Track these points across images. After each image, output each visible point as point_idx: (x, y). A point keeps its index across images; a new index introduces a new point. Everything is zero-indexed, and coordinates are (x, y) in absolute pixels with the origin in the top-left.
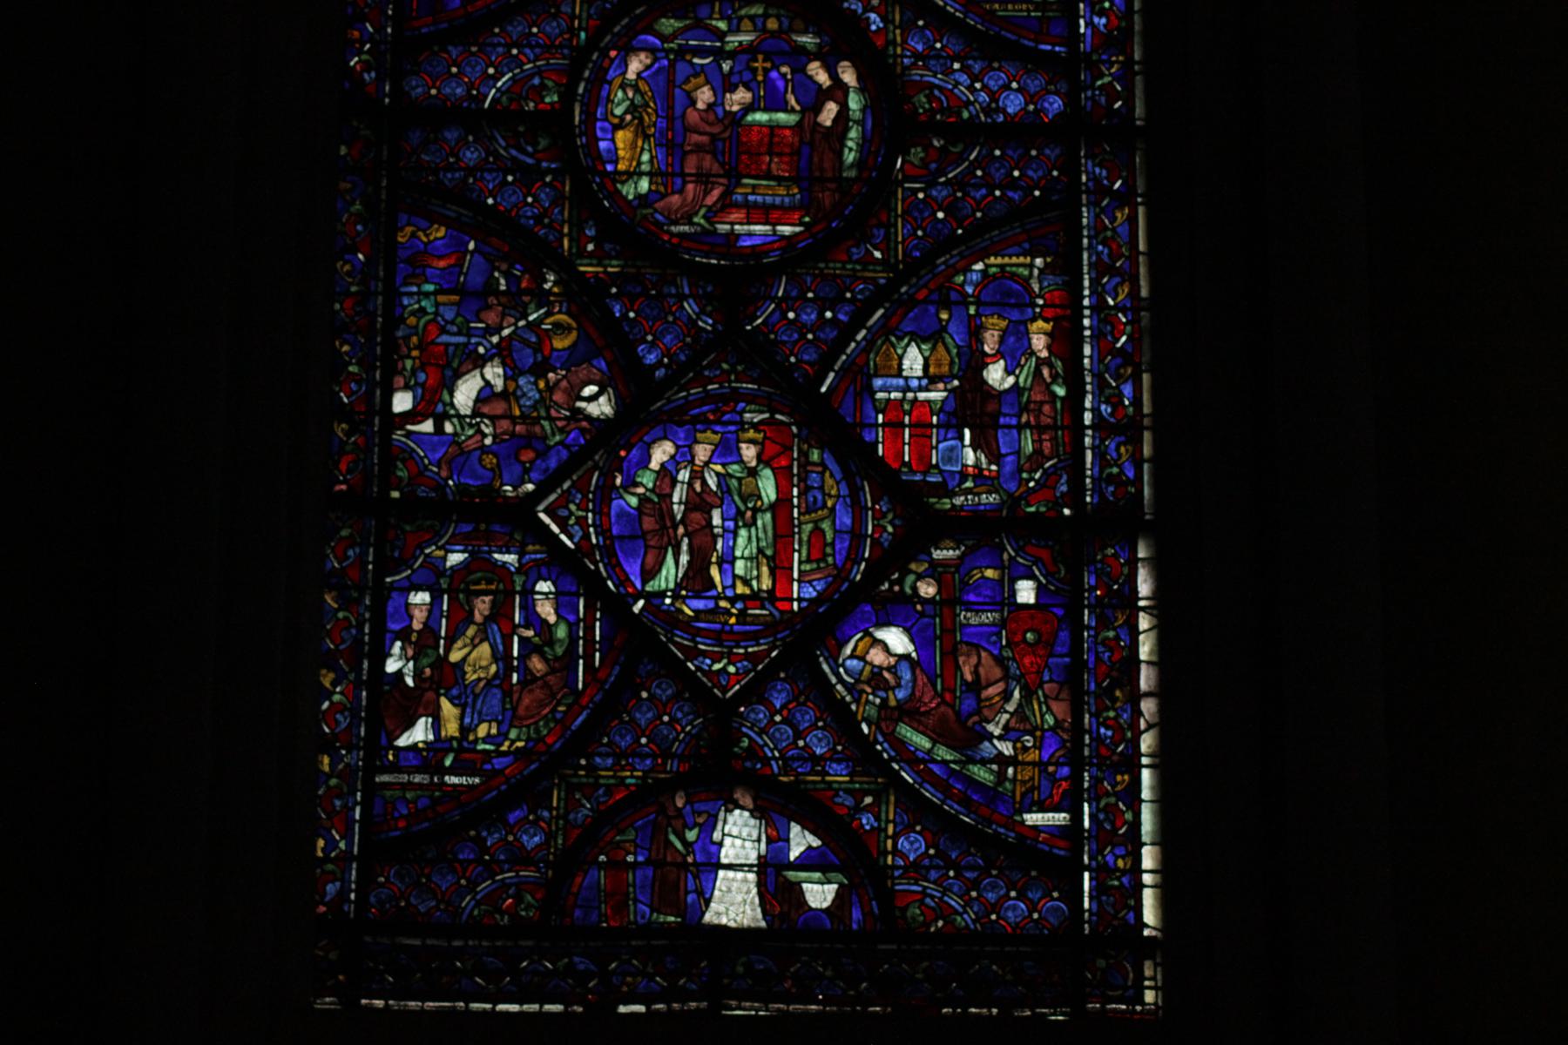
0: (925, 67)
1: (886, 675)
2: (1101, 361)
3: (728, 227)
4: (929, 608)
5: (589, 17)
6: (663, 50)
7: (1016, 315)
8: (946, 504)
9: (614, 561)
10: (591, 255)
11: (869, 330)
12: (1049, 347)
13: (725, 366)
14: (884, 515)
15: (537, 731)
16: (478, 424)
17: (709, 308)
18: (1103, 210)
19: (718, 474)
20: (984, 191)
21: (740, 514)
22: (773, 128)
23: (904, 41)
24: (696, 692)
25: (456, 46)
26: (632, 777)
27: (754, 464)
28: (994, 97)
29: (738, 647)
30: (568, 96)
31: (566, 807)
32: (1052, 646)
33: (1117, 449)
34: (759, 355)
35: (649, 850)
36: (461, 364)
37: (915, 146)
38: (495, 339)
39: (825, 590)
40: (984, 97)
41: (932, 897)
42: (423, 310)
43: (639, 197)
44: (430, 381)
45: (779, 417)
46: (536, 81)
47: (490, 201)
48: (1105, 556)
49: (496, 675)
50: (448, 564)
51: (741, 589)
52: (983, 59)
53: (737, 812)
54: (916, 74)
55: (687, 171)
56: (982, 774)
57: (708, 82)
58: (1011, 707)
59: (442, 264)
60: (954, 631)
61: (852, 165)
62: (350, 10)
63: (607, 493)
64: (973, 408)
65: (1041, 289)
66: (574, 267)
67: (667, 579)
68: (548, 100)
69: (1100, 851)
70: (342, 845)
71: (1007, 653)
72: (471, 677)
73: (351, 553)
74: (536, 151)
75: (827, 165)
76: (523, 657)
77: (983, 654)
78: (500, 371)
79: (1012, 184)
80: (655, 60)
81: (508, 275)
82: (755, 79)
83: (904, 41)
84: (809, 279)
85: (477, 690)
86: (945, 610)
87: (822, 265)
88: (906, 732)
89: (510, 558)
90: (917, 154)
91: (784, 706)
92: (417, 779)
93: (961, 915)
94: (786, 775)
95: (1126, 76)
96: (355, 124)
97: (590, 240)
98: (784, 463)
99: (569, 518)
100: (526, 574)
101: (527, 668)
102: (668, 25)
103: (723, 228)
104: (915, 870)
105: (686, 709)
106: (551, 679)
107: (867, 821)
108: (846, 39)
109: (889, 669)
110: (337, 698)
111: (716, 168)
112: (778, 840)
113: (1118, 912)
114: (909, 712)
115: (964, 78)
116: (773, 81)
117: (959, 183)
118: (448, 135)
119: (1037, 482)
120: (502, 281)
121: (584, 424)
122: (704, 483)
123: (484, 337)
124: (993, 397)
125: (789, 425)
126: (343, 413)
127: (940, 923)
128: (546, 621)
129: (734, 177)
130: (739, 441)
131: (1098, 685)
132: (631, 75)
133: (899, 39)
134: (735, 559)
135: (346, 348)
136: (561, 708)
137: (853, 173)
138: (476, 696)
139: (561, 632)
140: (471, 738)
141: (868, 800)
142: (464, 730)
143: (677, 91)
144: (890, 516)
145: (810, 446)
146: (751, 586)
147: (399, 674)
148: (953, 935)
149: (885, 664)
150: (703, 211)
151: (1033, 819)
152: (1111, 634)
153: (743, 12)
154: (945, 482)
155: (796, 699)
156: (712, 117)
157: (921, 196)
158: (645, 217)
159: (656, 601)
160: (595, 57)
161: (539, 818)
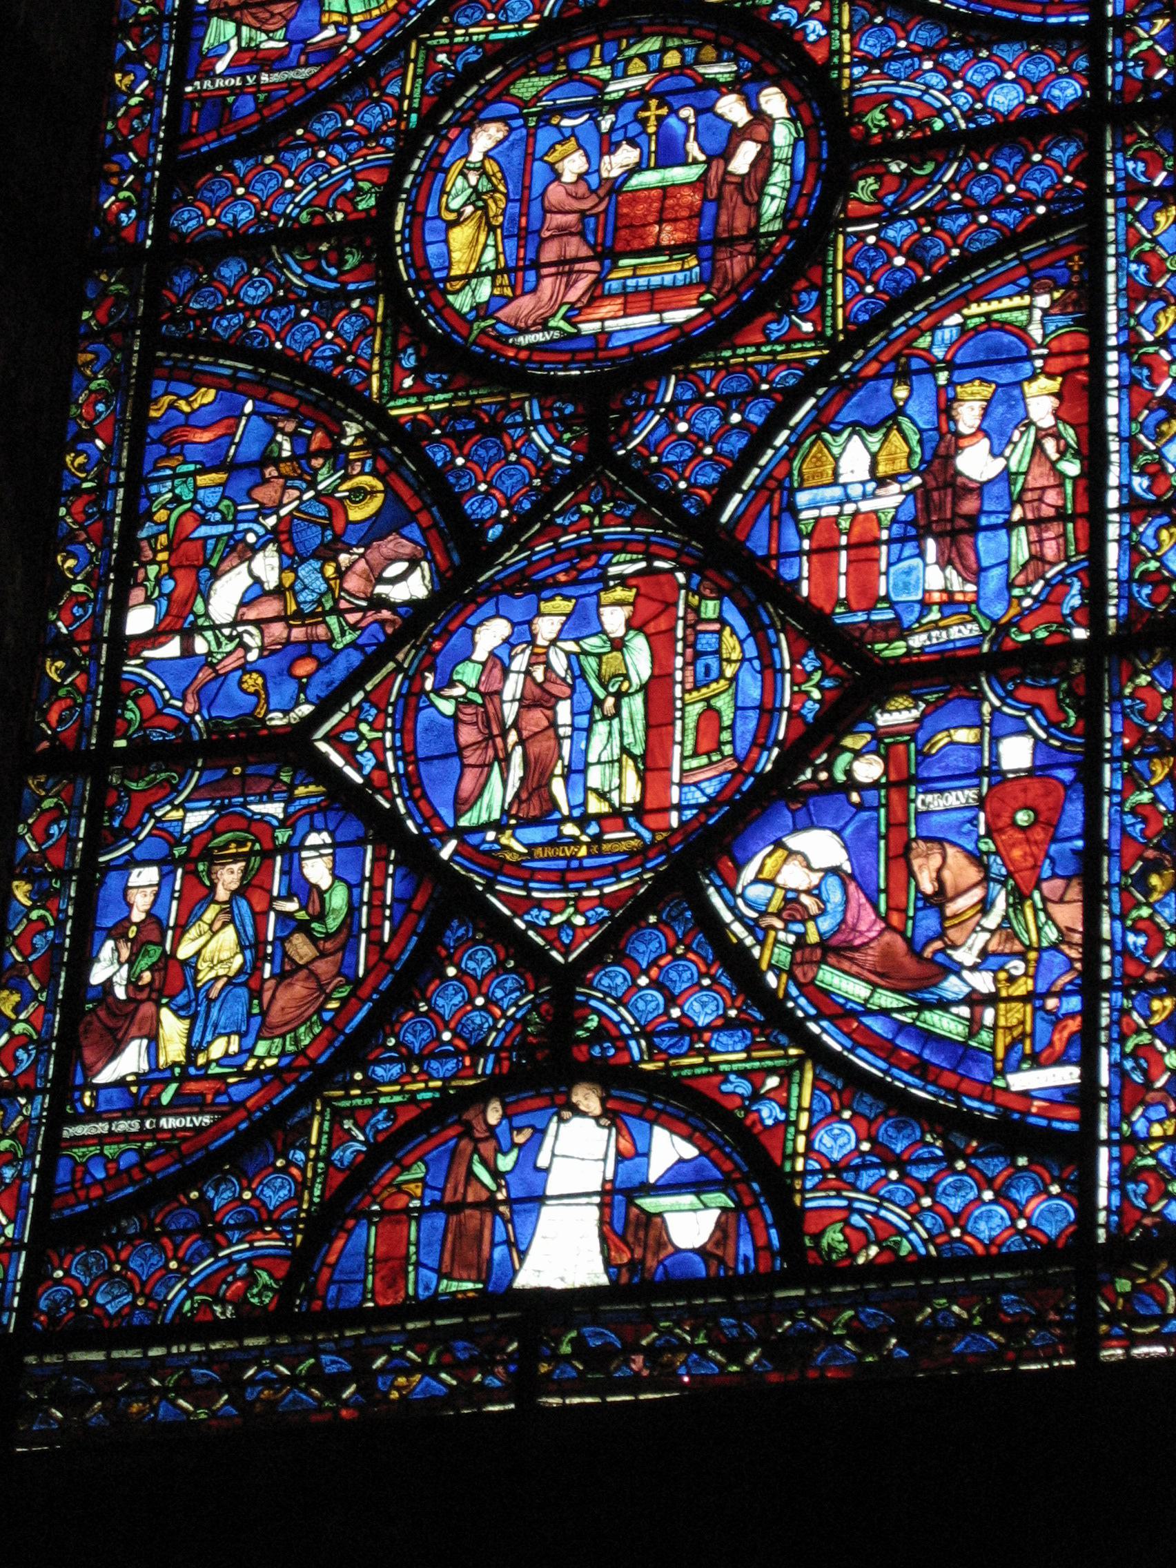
0: (884, 75)
1: (805, 899)
2: (1133, 418)
3: (598, 325)
4: (871, 796)
5: (424, 93)
7: (1006, 376)
8: (899, 649)
9: (417, 792)
10: (408, 393)
11: (793, 430)
12: (1056, 414)
13: (586, 508)
14: (808, 676)
15: (296, 1041)
16: (240, 635)
17: (567, 436)
18: (1137, 217)
19: (568, 654)
20: (963, 220)
21: (598, 702)
22: (666, 191)
24: (526, 958)
26: (427, 1089)
27: (620, 632)
29: (590, 886)
31: (329, 1145)
32: (1056, 827)
33: (1156, 536)
34: (642, 487)
35: (443, 1190)
36: (222, 560)
37: (864, 177)
38: (271, 521)
39: (719, 793)
40: (964, 100)
41: (862, 1213)
42: (177, 500)
44: (181, 589)
45: (658, 564)
46: (349, 185)
47: (278, 346)
48: (1137, 688)
49: (241, 971)
50: (187, 828)
51: (596, 806)
52: (965, 46)
53: (577, 1121)
54: (868, 87)
56: (947, 1024)
57: (580, 147)
58: (992, 921)
59: (206, 436)
60: (907, 824)
61: (775, 217)
63: (413, 698)
64: (943, 511)
65: (1045, 336)
66: (383, 409)
67: (489, 807)
68: (361, 206)
69: (1126, 1116)
70: (9, 1231)
71: (987, 845)
72: (205, 976)
73: (54, 830)
76: (281, 940)
77: (951, 851)
78: (275, 561)
79: (1007, 203)
80: (511, 130)
81: (293, 436)
82: (644, 131)
85: (213, 994)
86: (895, 796)
88: (829, 977)
89: (276, 809)
90: (866, 188)
91: (654, 963)
92: (122, 1126)
93: (903, 1234)
94: (651, 1060)
96: (104, 278)
98: (662, 624)
99: (358, 742)
100: (293, 827)
101: (285, 954)
102: (526, 88)
103: (588, 328)
104: (839, 1172)
105: (509, 984)
106: (323, 967)
107: (769, 1113)
108: (773, 55)
109: (808, 892)
110: (18, 1028)
111: (585, 251)
112: (636, 1154)
113: (1150, 1205)
114: (834, 949)
115: (936, 79)
118: (225, 272)
119: (1035, 598)
120: (287, 446)
121: (386, 614)
122: (548, 668)
123: (256, 521)
124: (971, 490)
125: (671, 571)
126: (61, 647)
127: (874, 1250)
128: (317, 887)
129: (607, 255)
130: (599, 605)
131: (1124, 873)
132: (476, 156)
133: (847, 47)
134: (587, 765)
135: (71, 563)
136: (333, 1005)
137: (777, 226)
138: (211, 1001)
139: (338, 899)
140: (201, 1060)
141: (773, 1082)
142: (192, 1051)
144: (817, 677)
145: (703, 597)
146: (609, 800)
147: (108, 984)
148: (895, 1266)
149: (803, 887)
150: (564, 309)
151: (1020, 1081)
152: (1146, 797)
153: (632, 52)
154: (898, 617)
155: (670, 950)
156: (582, 189)
157: (871, 240)
158: (483, 331)
159: (474, 839)
161: (290, 1163)
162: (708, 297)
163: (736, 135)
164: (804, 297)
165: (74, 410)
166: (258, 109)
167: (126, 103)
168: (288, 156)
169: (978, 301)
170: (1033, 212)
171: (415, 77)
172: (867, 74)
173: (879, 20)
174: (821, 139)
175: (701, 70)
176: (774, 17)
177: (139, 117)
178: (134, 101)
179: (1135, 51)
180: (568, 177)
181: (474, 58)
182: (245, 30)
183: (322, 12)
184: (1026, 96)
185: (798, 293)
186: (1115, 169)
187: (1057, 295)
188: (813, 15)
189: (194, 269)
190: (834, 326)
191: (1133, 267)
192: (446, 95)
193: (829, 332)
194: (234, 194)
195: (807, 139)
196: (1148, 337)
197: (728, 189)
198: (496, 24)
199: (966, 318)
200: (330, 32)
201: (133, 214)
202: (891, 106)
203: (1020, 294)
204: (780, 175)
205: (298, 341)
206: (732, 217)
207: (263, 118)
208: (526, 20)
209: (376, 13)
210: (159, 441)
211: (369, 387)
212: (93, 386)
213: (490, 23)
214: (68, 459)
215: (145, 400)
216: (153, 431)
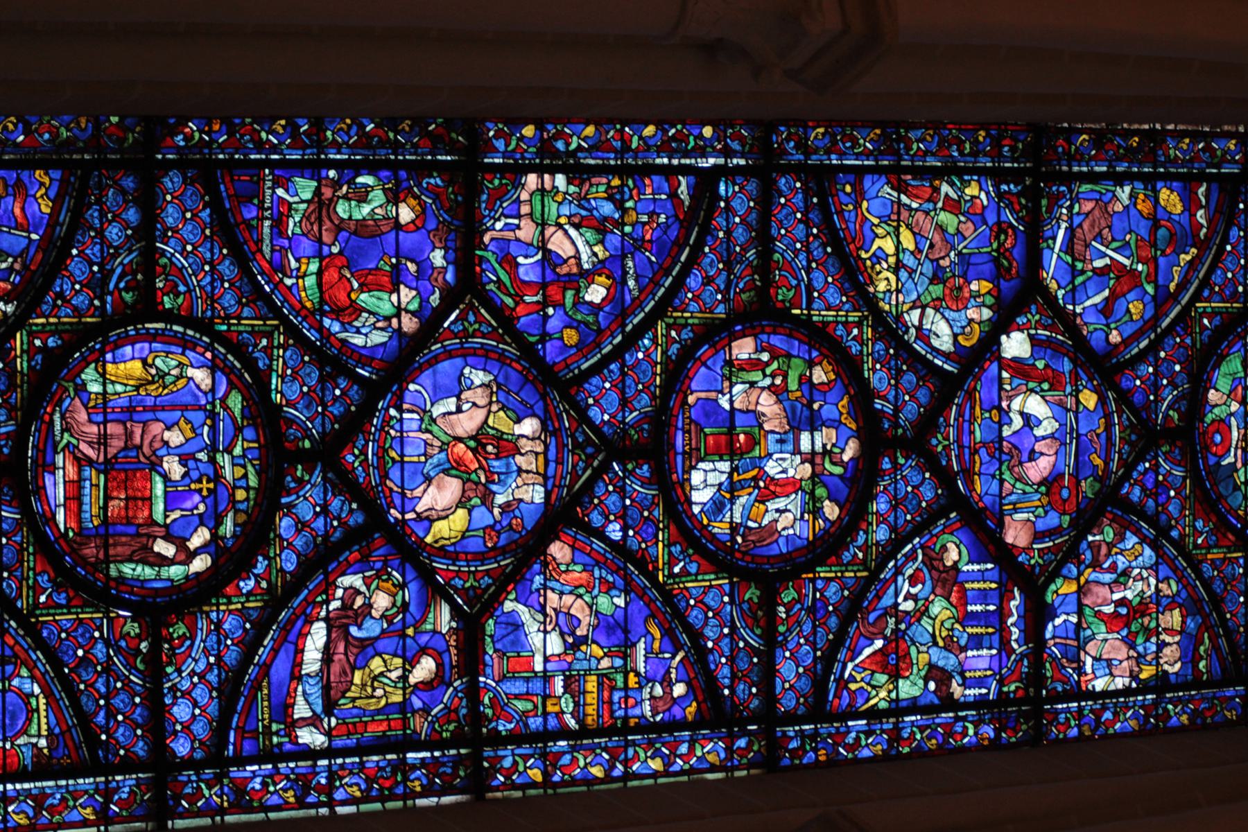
0: (209, 632)
3: (61, 465)
5: (241, 333)
6: (214, 399)
10: (31, 343)
18: (92, 796)
20: (103, 690)
22: (149, 500)
23: (231, 612)
25: (210, 216)
28: (187, 694)
30: (169, 317)
37: (140, 627)
40: (186, 685)
43: (84, 384)
46: (182, 288)
52: (219, 682)
54: (202, 624)
55: (109, 425)
57: (187, 440)
59: (17, 211)
61: (120, 572)
62: (237, 121)
65: (19, 746)
66: (20, 328)
68: (166, 299)
74: (120, 291)
75: (119, 549)
79: (111, 713)
80: (205, 393)
82: (192, 481)
83: (231, 612)
84: (18, 539)
87: (31, 550)
90: (133, 628)
95: (212, 810)
97: (45, 343)
102: (236, 402)
103: (59, 460)
111: (112, 451)
115: (201, 666)
116: (191, 498)
117: (109, 669)
118: (132, 212)
129: (107, 467)
132: (191, 372)
133: (232, 607)
137: (113, 573)
143: (179, 413)
150: (74, 441)
153: (250, 468)
156: (157, 445)
157: (97, 634)
158: (67, 390)
160: (205, 339)
162: (71, 534)
163: (180, 542)
164: (64, 595)
165: (47, 118)
166: (247, 223)
167: (263, 129)
168: (208, 245)
169: (47, 704)
170: (103, 732)
171: (253, 326)
172: (212, 621)
173: (248, 626)
174: (170, 596)
175: (230, 515)
176: (260, 558)
177: (251, 140)
178: (264, 135)
179: (203, 786)
180: (167, 435)
181: (261, 364)
182: (304, 206)
183: (309, 258)
184: (181, 723)
185: (66, 592)
186: (124, 780)
187: (45, 751)
188: (257, 583)
189: (135, 190)
190: (42, 615)
191: (58, 796)
192: (238, 349)
193: (38, 612)
194: (187, 211)
195: (174, 588)
196: (10, 809)
197: (144, 540)
198: (283, 377)
199: (37, 697)
200: (294, 264)
201: (182, 143)
202: (187, 638)
203: (49, 729)
204: (149, 572)
205: (76, 267)
206: (123, 544)
207: (237, 225)
208: (283, 395)
209: (303, 294)
210: (19, 179)
211: (38, 317)
212: (63, 130)
213: (284, 371)
214: (12, 119)
215: (46, 166)
216: (25, 175)
